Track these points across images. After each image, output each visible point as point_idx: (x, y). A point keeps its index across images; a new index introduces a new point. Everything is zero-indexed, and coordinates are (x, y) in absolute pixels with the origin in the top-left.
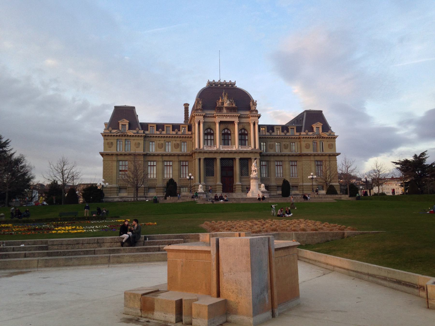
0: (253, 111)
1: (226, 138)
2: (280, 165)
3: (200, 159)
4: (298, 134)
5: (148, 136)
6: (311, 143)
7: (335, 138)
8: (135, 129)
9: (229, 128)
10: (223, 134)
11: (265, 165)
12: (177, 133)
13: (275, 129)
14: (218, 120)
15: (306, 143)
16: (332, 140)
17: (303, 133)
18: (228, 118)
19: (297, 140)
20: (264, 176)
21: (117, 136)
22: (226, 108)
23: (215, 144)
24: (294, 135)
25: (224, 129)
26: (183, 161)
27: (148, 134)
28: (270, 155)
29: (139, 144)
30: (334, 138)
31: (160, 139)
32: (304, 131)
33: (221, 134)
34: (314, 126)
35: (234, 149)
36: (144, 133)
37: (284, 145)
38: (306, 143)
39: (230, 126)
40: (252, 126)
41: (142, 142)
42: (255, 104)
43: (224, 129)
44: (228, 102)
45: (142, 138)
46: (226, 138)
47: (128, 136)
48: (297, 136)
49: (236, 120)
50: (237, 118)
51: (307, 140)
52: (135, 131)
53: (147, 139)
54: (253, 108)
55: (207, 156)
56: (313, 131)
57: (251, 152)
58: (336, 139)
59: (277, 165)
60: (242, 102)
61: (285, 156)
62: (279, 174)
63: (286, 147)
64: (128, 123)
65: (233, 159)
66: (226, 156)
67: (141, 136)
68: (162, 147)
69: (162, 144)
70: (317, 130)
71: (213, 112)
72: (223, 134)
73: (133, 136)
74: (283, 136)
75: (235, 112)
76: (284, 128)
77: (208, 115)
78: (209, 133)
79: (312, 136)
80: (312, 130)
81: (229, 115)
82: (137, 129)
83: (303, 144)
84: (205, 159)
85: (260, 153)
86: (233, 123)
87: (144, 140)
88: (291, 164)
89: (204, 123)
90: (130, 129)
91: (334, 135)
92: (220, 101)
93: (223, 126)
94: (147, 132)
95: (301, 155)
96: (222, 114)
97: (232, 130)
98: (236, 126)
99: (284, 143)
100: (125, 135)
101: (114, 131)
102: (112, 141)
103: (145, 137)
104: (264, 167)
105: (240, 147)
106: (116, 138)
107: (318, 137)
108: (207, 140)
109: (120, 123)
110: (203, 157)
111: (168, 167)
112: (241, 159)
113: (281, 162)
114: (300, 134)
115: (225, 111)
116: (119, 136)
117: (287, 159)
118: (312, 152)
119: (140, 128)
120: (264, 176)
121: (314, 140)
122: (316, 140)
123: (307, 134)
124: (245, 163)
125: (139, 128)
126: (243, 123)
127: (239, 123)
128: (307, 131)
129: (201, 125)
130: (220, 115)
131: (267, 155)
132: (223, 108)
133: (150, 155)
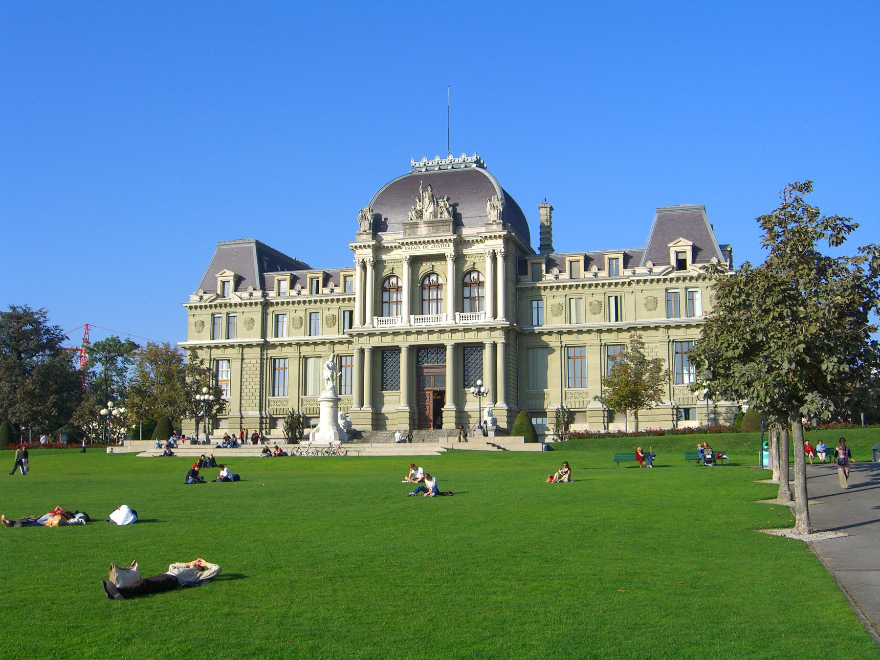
0: (491, 224)
1: (421, 295)
3: (362, 351)
8: (246, 290)
9: (436, 270)
15: (646, 294)
18: (430, 246)
21: (211, 306)
22: (425, 223)
29: (252, 320)
38: (646, 294)
39: (438, 266)
40: (488, 261)
47: (231, 305)
50: (452, 245)
52: (245, 295)
56: (669, 264)
61: (589, 332)
64: (690, 248)
66: (423, 340)
67: (256, 304)
73: (241, 305)
75: (448, 231)
79: (661, 277)
81: (430, 239)
82: (250, 289)
84: (375, 350)
86: (442, 257)
96: (413, 240)
98: (450, 264)
100: (226, 306)
101: (206, 297)
102: (202, 318)
106: (209, 311)
109: (219, 279)
110: (368, 344)
112: (457, 347)
115: (423, 230)
116: (216, 306)
119: (258, 287)
125: (253, 284)
126: (471, 255)
128: (649, 264)
132: (417, 224)
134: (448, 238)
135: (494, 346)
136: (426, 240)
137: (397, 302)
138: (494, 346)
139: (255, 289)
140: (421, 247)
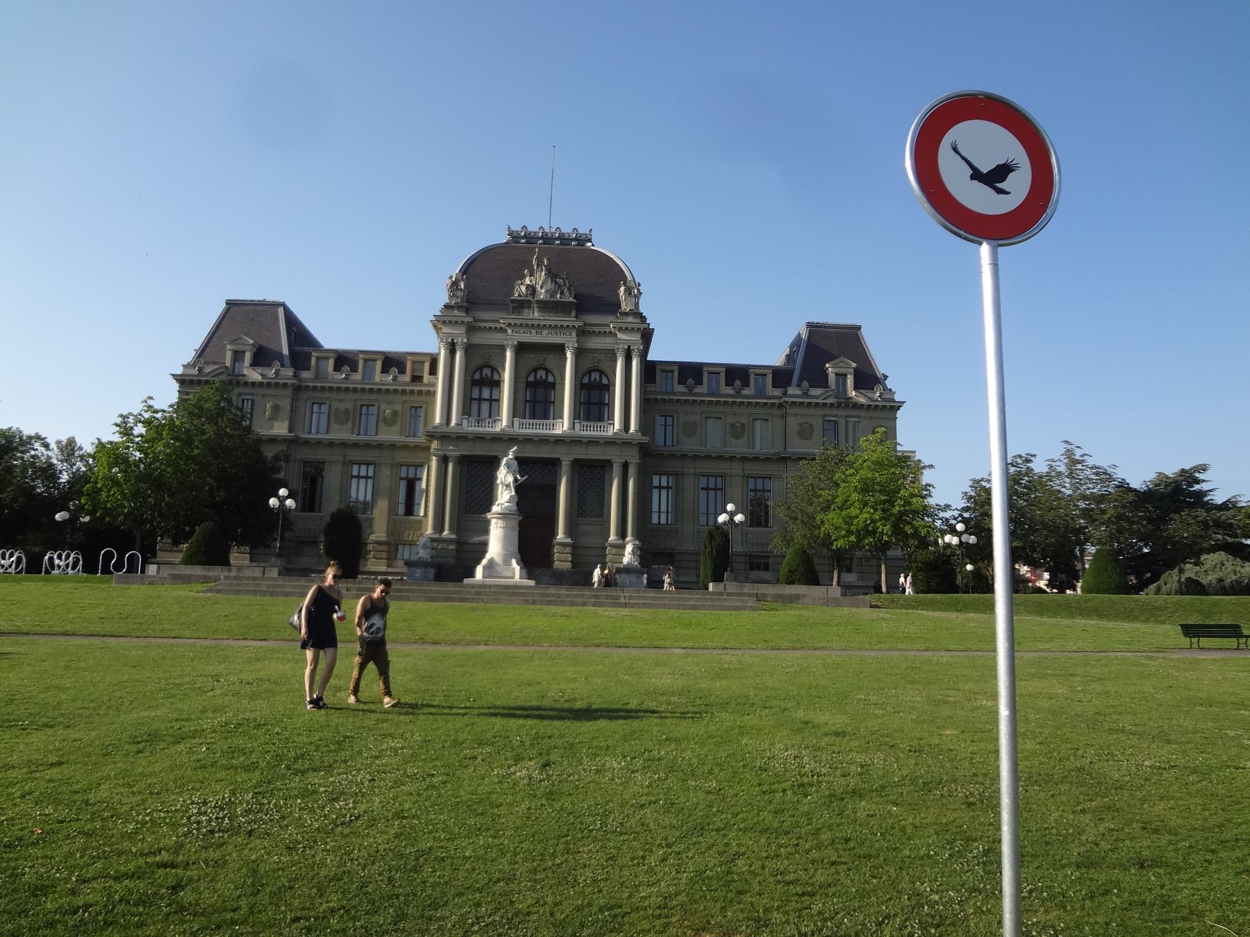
1: (536, 396)
2: (716, 489)
4: (777, 392)
5: (307, 387)
6: (817, 423)
7: (894, 407)
9: (548, 365)
10: (529, 385)
11: (668, 488)
12: (395, 379)
13: (705, 376)
14: (514, 337)
16: (885, 414)
17: (793, 390)
18: (545, 332)
19: (775, 411)
20: (663, 521)
22: (538, 302)
23: (494, 414)
24: (672, 393)
25: (535, 370)
26: (360, 464)
27: (308, 380)
28: (684, 457)
30: (892, 407)
31: (342, 395)
32: (799, 385)
33: (522, 386)
34: (830, 369)
35: (558, 430)
36: (295, 376)
37: (732, 425)
39: (551, 361)
41: (286, 404)
42: (634, 292)
43: (535, 370)
44: (549, 285)
45: (289, 392)
46: (536, 396)
48: (774, 397)
49: (570, 342)
50: (574, 334)
51: (803, 411)
53: (305, 395)
54: (625, 306)
55: (468, 449)
56: (827, 386)
57: (610, 442)
58: (899, 414)
59: (707, 489)
60: (591, 286)
61: (732, 458)
62: (663, 517)
63: (737, 431)
65: (554, 463)
67: (285, 385)
68: (347, 419)
69: (347, 411)
70: (837, 382)
71: (503, 319)
72: (529, 385)
73: (261, 384)
74: (682, 394)
76: (780, 376)
77: (483, 325)
78: (481, 380)
79: (820, 401)
80: (822, 380)
81: (547, 323)
83: (793, 423)
85: (645, 451)
87: (295, 400)
88: (751, 486)
89: (469, 349)
90: (255, 364)
91: (893, 401)
92: (527, 281)
93: (532, 360)
94: (305, 375)
95: (783, 459)
97: (556, 373)
99: (732, 420)
103: (298, 389)
104: (664, 492)
105: (577, 426)
107: (839, 404)
108: (480, 400)
111: (362, 481)
113: (719, 479)
114: (785, 394)
117: (737, 468)
118: (403, 439)
120: (663, 521)
121: (828, 412)
122: (835, 412)
123: (806, 395)
124: (591, 475)
126: (594, 351)
127: (579, 353)
128: (805, 384)
129: (458, 356)
130: (518, 322)
131: (672, 456)
133: (307, 443)
134: (571, 324)
135: (625, 466)
136: (542, 323)
137: (491, 400)
138: (625, 466)
139: (283, 366)
140: (534, 332)
